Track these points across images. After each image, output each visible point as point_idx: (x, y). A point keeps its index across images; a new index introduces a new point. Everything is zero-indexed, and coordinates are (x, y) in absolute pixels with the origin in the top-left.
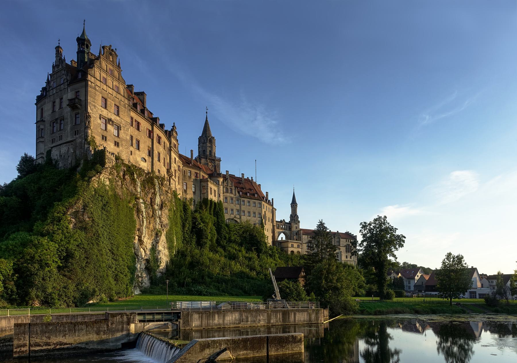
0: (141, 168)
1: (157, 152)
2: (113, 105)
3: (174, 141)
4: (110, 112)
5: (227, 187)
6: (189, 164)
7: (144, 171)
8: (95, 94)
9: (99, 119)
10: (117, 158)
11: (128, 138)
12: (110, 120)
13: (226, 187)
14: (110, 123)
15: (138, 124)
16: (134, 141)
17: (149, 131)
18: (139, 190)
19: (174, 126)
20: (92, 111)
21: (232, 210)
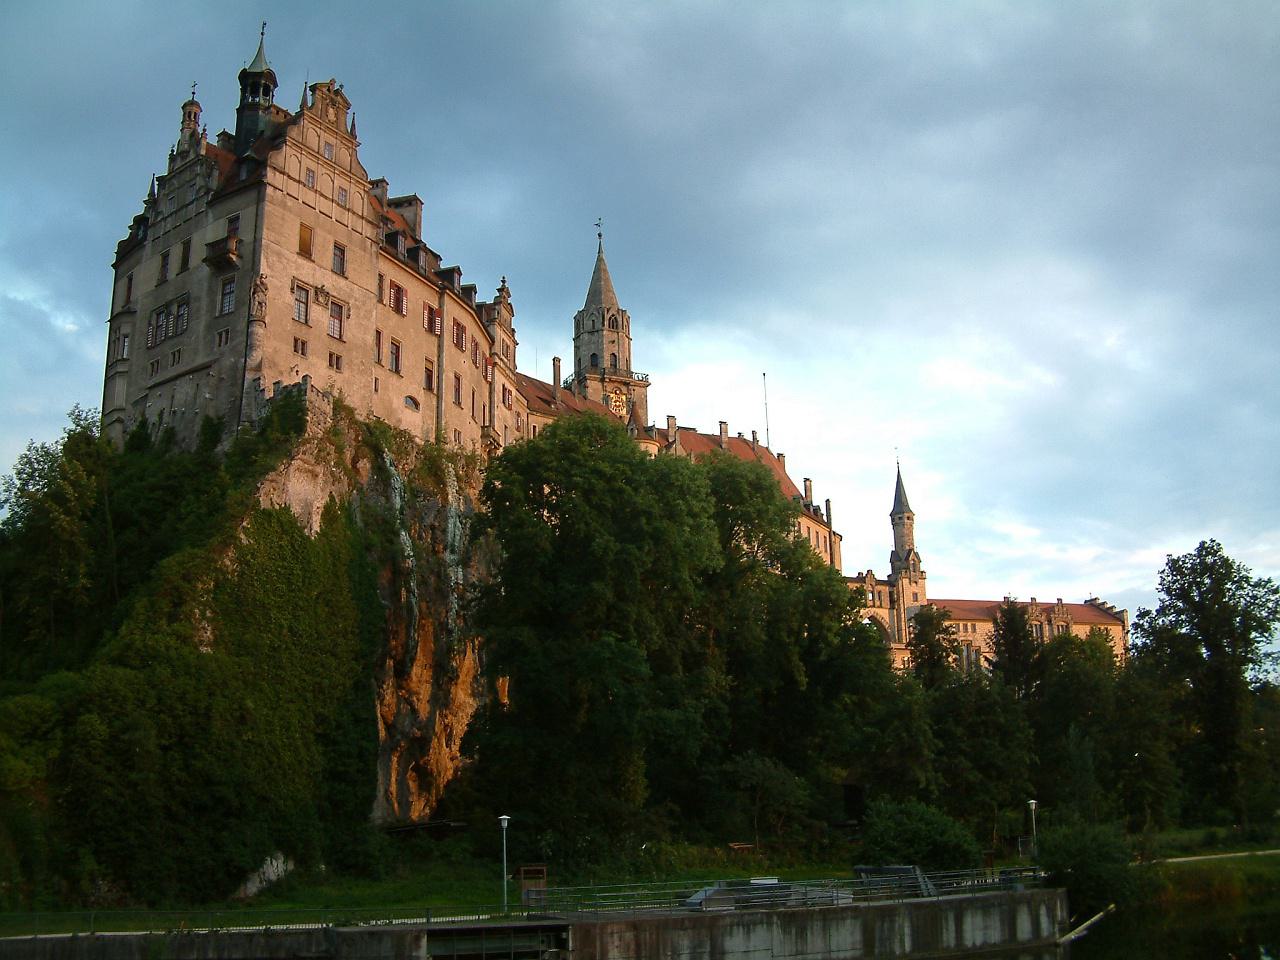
0: (405, 431)
1: (452, 376)
2: (332, 247)
3: (504, 336)
6: (549, 403)
7: (411, 439)
8: (283, 219)
10: (339, 406)
11: (371, 338)
12: (319, 291)
14: (320, 299)
15: (399, 291)
16: (386, 348)
17: (431, 310)
18: (398, 502)
20: (272, 270)
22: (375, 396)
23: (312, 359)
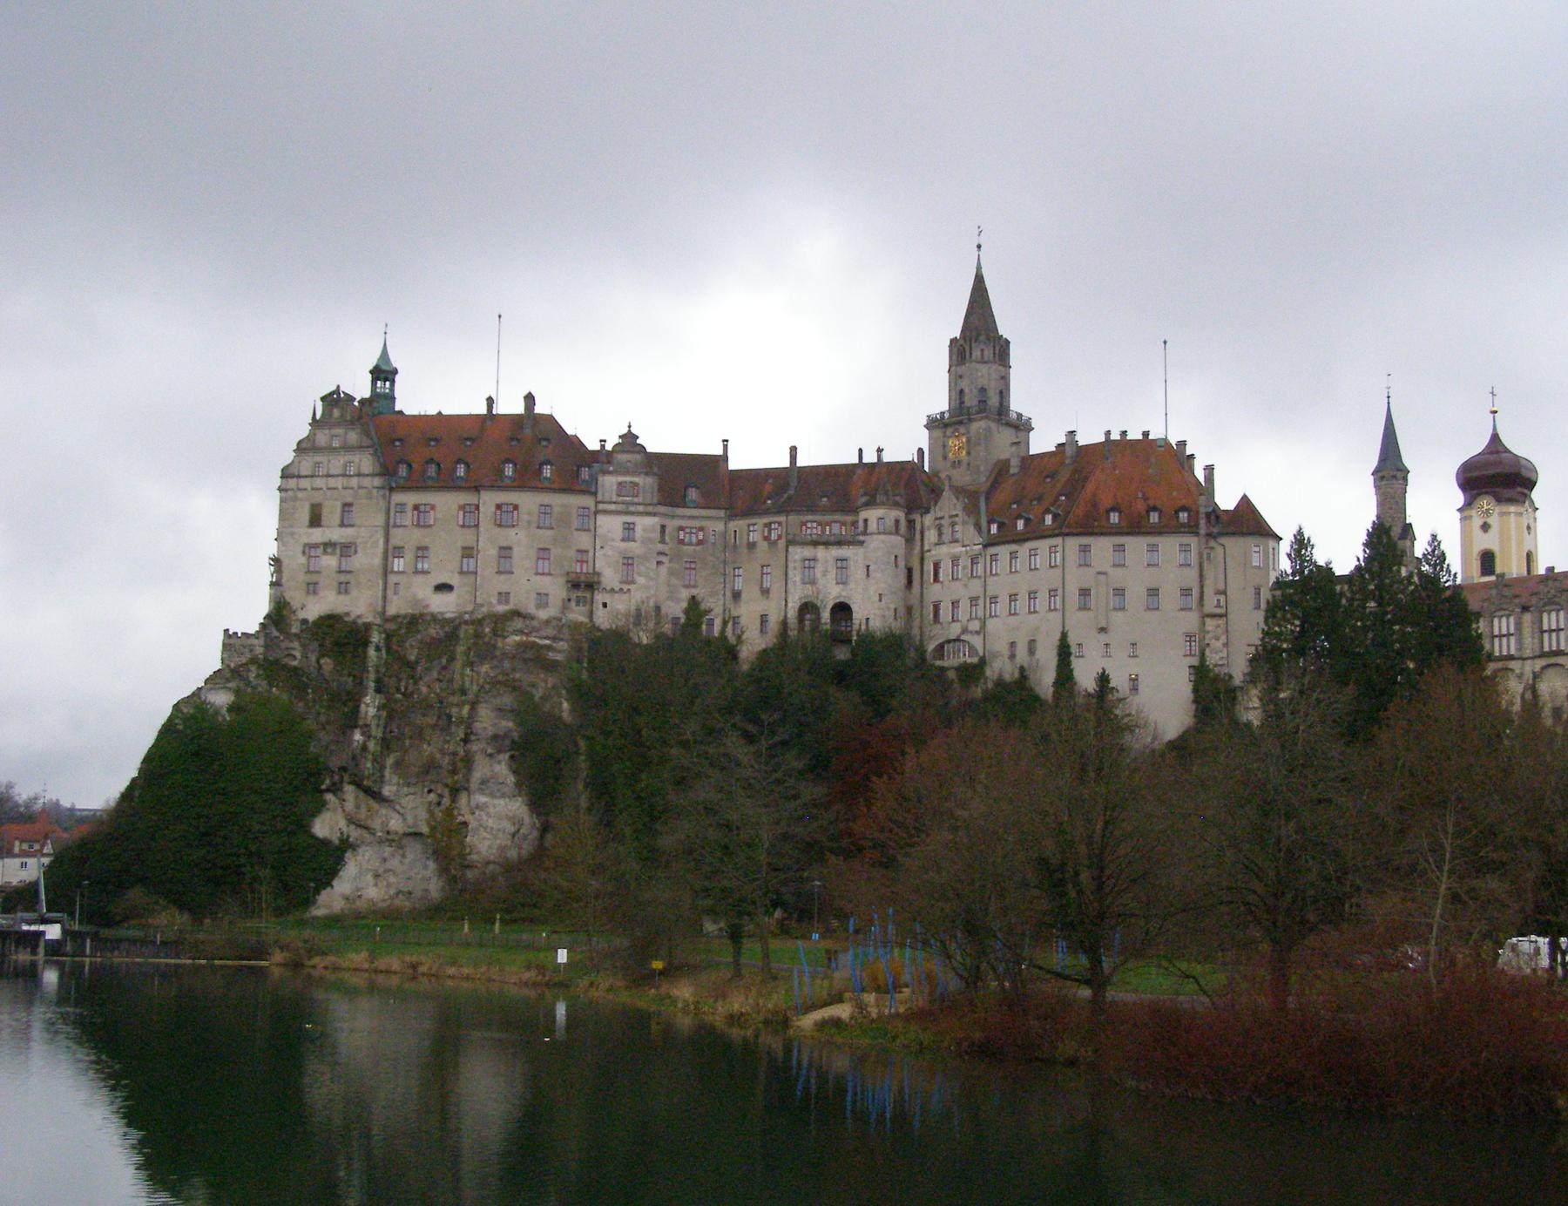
4: (328, 527)
5: (942, 522)
8: (294, 508)
9: (300, 555)
13: (938, 522)
21: (955, 604)
22: (395, 598)
23: (322, 594)
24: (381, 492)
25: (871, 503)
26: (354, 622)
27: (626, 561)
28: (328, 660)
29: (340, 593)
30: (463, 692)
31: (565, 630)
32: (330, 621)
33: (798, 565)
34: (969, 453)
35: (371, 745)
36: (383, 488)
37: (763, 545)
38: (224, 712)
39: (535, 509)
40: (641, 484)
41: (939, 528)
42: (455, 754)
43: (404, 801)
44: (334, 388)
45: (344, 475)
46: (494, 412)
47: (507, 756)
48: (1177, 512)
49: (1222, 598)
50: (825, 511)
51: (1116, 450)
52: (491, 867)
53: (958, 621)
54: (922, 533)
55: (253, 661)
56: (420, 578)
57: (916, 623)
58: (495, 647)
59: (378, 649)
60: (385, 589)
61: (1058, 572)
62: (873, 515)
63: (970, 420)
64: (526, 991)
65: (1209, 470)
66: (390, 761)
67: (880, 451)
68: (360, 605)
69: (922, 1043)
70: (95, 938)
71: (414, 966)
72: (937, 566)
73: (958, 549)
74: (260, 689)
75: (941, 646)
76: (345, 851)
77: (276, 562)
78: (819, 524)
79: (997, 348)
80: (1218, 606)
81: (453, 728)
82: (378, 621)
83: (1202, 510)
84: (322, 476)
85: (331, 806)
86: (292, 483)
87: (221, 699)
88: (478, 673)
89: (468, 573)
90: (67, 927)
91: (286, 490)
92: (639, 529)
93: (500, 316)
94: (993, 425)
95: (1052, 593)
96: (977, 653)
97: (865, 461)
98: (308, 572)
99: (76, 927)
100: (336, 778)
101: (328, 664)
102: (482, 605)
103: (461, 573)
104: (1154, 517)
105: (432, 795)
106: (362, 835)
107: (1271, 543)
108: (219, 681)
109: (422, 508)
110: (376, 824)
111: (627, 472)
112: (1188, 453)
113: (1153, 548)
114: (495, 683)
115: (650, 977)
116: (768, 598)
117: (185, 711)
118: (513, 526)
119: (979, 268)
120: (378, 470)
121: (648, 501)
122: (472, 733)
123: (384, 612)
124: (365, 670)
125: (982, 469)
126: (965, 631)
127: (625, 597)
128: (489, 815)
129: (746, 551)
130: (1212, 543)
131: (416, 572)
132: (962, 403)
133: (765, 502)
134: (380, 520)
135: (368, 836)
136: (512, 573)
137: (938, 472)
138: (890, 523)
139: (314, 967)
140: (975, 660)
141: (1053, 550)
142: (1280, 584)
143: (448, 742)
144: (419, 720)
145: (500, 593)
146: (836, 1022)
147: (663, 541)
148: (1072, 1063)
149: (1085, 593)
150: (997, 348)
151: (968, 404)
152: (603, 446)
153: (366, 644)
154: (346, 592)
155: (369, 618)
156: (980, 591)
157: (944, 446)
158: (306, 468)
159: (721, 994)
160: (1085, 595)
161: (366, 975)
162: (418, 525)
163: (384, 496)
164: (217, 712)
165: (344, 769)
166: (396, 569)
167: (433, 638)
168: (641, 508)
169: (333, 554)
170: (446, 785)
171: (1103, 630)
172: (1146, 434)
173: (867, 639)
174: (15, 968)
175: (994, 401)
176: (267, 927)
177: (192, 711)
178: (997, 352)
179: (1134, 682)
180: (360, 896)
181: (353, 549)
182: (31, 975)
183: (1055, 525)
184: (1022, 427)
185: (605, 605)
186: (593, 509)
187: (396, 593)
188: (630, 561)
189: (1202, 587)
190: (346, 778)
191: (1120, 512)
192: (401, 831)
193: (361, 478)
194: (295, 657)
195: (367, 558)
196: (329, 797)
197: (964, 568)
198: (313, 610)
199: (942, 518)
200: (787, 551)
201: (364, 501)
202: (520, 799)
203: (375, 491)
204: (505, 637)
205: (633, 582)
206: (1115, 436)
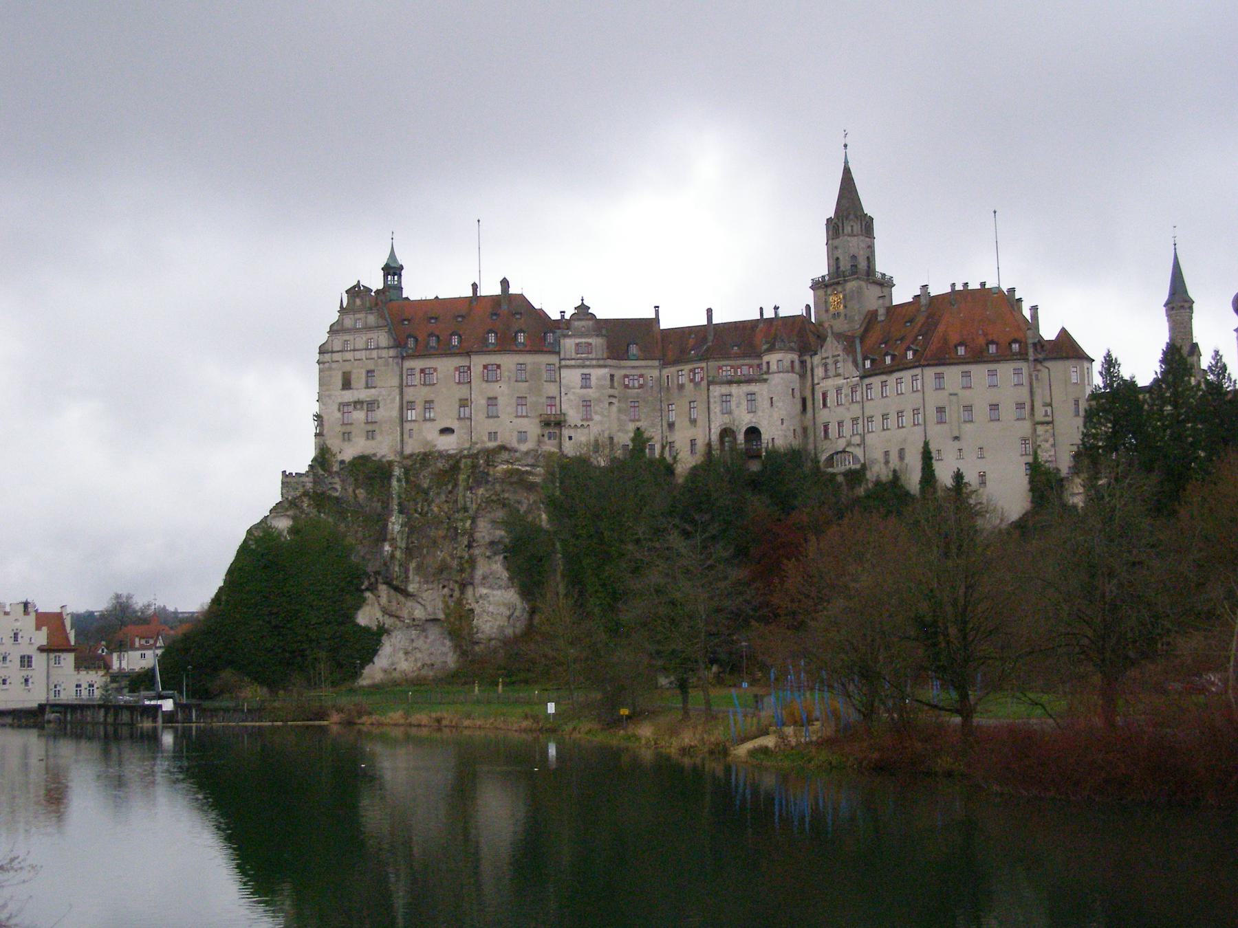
4: (357, 389)
5: (828, 361)
8: (331, 376)
13: (824, 361)
14: (358, 407)
19: (583, 303)
21: (840, 424)
24: (395, 361)
25: (771, 349)
26: (380, 460)
27: (585, 403)
28: (362, 491)
29: (368, 438)
30: (466, 509)
31: (541, 459)
32: (362, 460)
33: (718, 399)
34: (845, 307)
35: (398, 554)
36: (397, 357)
37: (689, 387)
38: (285, 533)
39: (513, 367)
40: (593, 344)
41: (825, 365)
42: (461, 558)
43: (424, 595)
44: (355, 283)
45: (367, 349)
46: (478, 295)
47: (501, 557)
48: (1010, 344)
49: (1049, 409)
50: (737, 357)
51: (961, 298)
52: (493, 642)
53: (843, 436)
54: (812, 370)
55: (305, 494)
56: (429, 424)
57: (811, 440)
58: (488, 474)
59: (399, 480)
60: (402, 434)
61: (920, 395)
62: (773, 358)
63: (846, 281)
64: (524, 736)
65: (1034, 309)
66: (413, 565)
67: (776, 308)
68: (384, 447)
69: (831, 763)
70: (198, 707)
71: (439, 721)
72: (825, 396)
73: (840, 381)
74: (311, 515)
75: (831, 457)
76: (382, 636)
77: (318, 417)
78: (732, 367)
79: (864, 224)
80: (1046, 415)
81: (460, 538)
82: (398, 459)
83: (1030, 341)
84: (350, 351)
85: (369, 601)
86: (327, 357)
87: (283, 524)
88: (476, 495)
89: (464, 418)
90: (178, 701)
91: (324, 363)
92: (593, 378)
93: (479, 221)
94: (863, 284)
95: (916, 411)
96: (859, 461)
97: (765, 316)
98: (343, 424)
99: (184, 701)
100: (373, 580)
101: (361, 493)
102: (476, 443)
103: (460, 419)
104: (992, 349)
105: (446, 590)
106: (394, 622)
107: (1086, 365)
108: (279, 510)
109: (427, 371)
110: (405, 614)
111: (582, 335)
112: (1017, 298)
113: (993, 373)
114: (489, 501)
115: (618, 722)
116: (695, 426)
117: (256, 534)
118: (497, 381)
119: (846, 162)
120: (391, 344)
121: (601, 357)
122: (474, 541)
123: (402, 452)
124: (390, 496)
125: (856, 318)
126: (849, 444)
127: (586, 431)
128: (489, 603)
129: (676, 391)
130: (1039, 367)
131: (425, 420)
132: (838, 268)
133: (690, 353)
134: (395, 382)
135: (398, 622)
136: (499, 417)
137: (823, 322)
138: (787, 364)
139: (363, 724)
140: (858, 466)
141: (914, 378)
142: (1095, 396)
143: (456, 548)
144: (433, 533)
145: (490, 433)
146: (764, 750)
147: (612, 387)
148: (949, 774)
149: (941, 410)
150: (864, 224)
151: (842, 268)
152: (563, 316)
153: (390, 476)
154: (373, 438)
155: (391, 457)
156: (859, 413)
157: (826, 302)
158: (337, 345)
159: (674, 732)
160: (941, 412)
161: (402, 729)
162: (425, 385)
163: (397, 363)
164: (280, 534)
165: (377, 573)
166: (409, 419)
167: (440, 470)
168: (594, 362)
169: (362, 409)
170: (456, 582)
171: (956, 438)
172: (983, 284)
173: (773, 454)
174: (142, 733)
175: (863, 265)
176: (326, 695)
177: (261, 535)
178: (863, 227)
179: (982, 476)
180: (395, 669)
181: (376, 405)
182: (152, 738)
183: (915, 359)
184: (886, 284)
185: (570, 438)
186: (557, 365)
187: (410, 436)
188: (588, 403)
189: (1032, 401)
190: (380, 580)
191: (966, 346)
192: (424, 618)
193: (380, 351)
194: (336, 490)
195: (388, 412)
196: (368, 594)
197: (846, 396)
198: (348, 453)
199: (828, 358)
200: (708, 389)
201: (383, 368)
202: (513, 590)
203: (391, 359)
204: (496, 467)
205: (591, 419)
206: (959, 287)
